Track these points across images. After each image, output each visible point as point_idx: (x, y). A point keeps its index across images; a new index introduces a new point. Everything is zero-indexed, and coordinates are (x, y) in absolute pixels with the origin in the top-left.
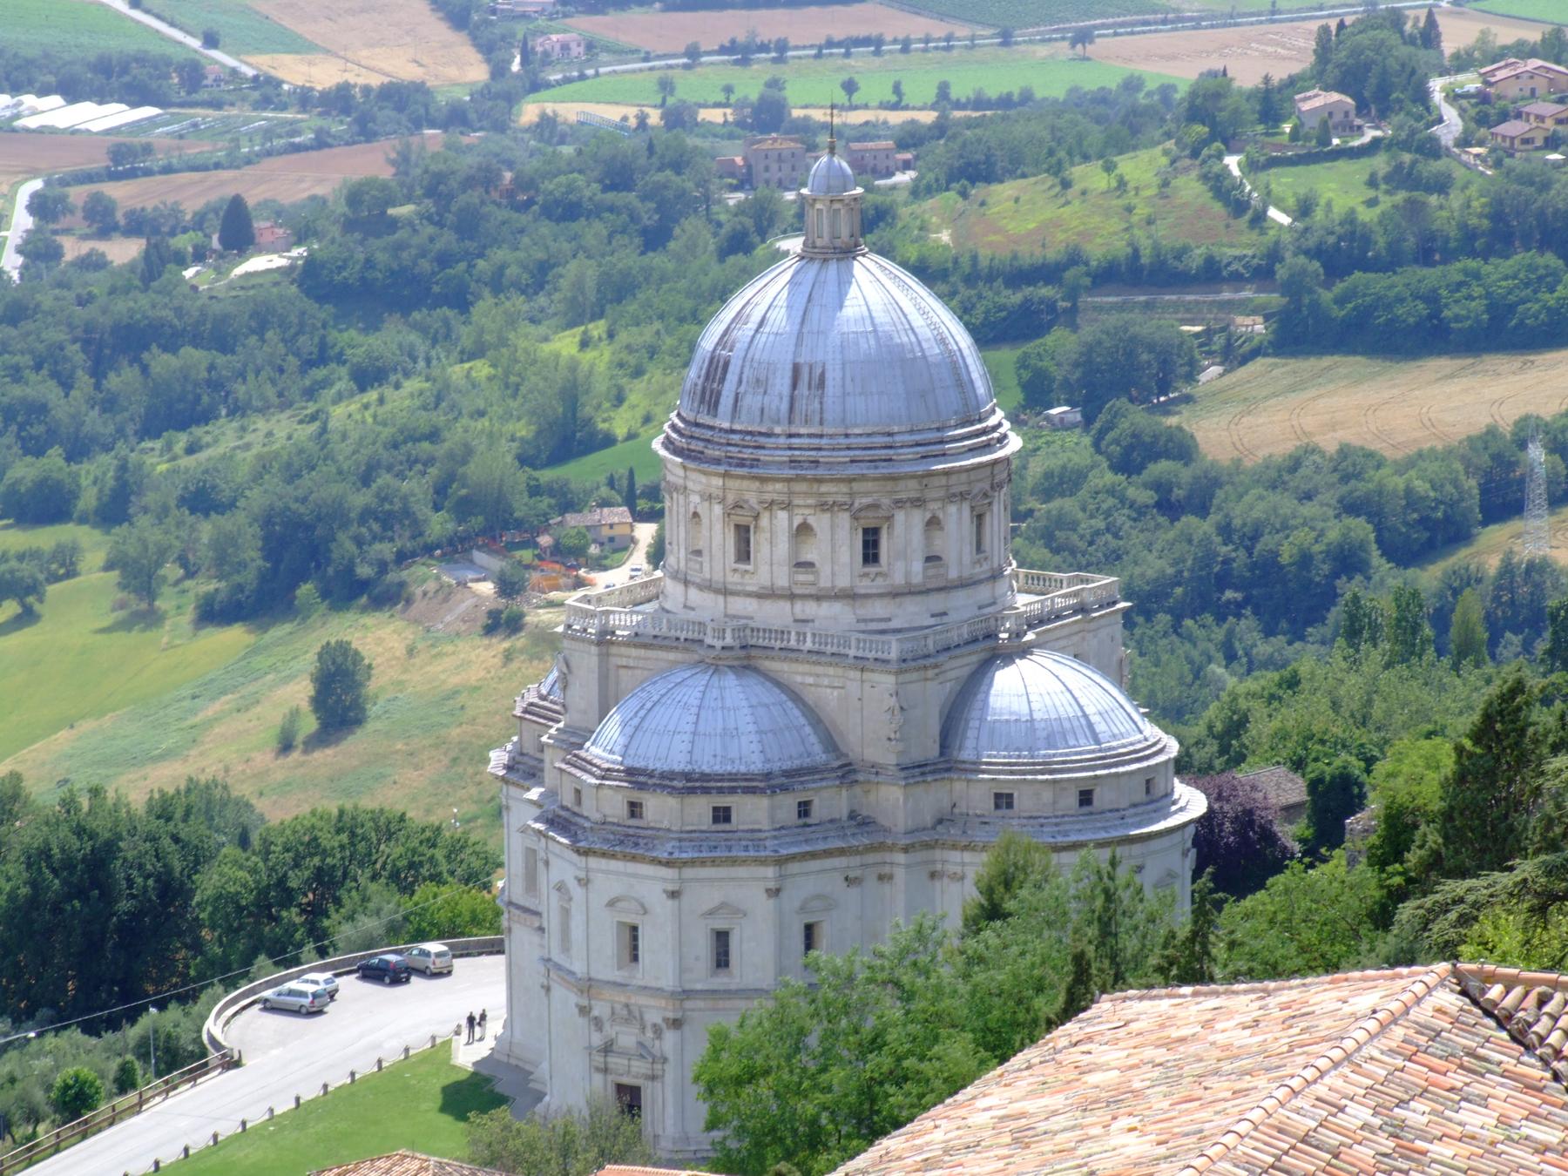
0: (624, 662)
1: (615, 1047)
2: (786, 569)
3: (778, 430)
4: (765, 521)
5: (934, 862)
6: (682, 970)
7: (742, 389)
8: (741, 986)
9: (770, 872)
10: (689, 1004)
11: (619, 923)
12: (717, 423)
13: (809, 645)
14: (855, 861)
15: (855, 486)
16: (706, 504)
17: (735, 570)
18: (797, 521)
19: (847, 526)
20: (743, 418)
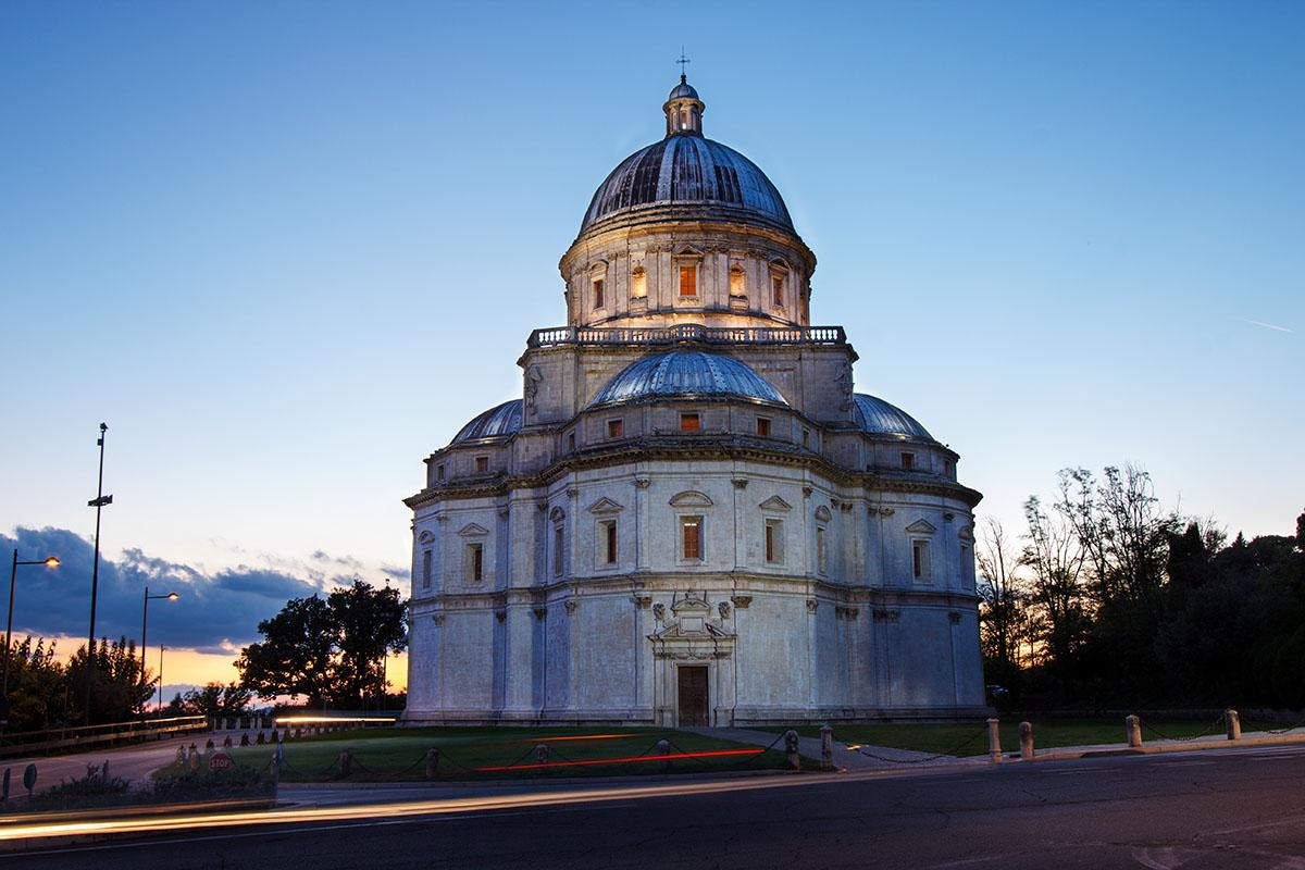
0: (593, 367)
2: (726, 297)
3: (712, 202)
4: (709, 261)
5: (871, 501)
6: (750, 554)
7: (677, 181)
8: (788, 573)
9: (807, 474)
10: (754, 585)
12: (658, 203)
14: (835, 488)
17: (682, 300)
19: (765, 270)
20: (681, 195)
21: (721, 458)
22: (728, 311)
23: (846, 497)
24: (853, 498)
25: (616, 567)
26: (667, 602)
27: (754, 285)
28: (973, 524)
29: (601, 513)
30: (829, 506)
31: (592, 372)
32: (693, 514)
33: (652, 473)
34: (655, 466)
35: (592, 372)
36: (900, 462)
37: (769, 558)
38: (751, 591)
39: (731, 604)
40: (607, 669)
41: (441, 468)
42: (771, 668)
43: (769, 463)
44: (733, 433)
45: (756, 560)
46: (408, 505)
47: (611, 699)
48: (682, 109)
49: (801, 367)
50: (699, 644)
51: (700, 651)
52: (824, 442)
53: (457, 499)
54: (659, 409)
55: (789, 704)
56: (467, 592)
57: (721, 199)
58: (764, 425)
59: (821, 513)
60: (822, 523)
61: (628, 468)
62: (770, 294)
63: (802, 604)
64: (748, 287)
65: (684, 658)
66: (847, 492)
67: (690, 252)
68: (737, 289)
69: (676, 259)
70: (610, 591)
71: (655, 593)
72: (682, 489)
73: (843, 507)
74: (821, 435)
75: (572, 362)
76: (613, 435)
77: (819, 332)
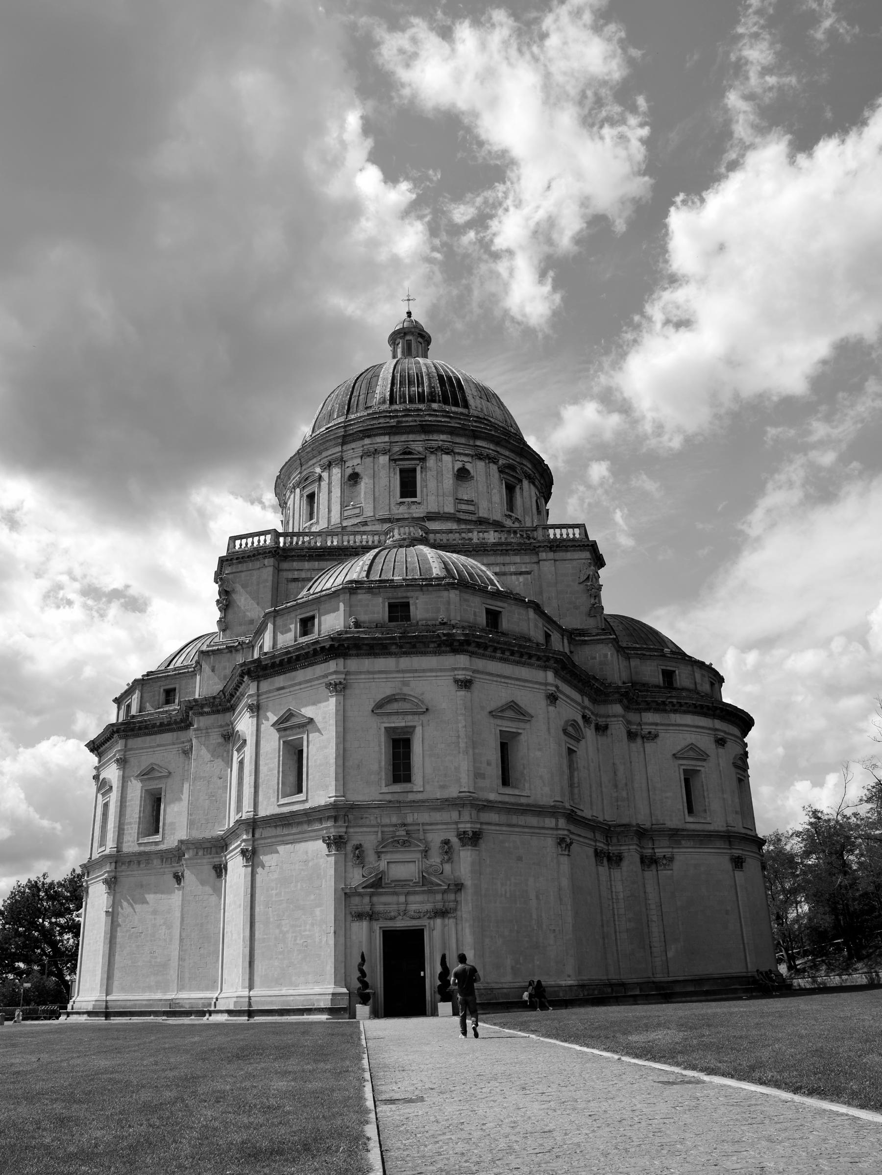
0: (296, 575)
1: (385, 881)
2: (451, 499)
4: (431, 461)
5: (629, 722)
6: (478, 775)
8: (530, 801)
10: (486, 816)
11: (385, 728)
13: (492, 540)
14: (587, 702)
15: (498, 449)
16: (371, 459)
18: (458, 465)
19: (497, 475)
21: (438, 652)
23: (601, 716)
24: (609, 716)
25: (305, 798)
26: (369, 840)
27: (482, 487)
28: (746, 754)
29: (285, 729)
31: (295, 580)
32: (403, 724)
33: (347, 673)
34: (353, 664)
35: (295, 580)
36: (659, 679)
37: (506, 781)
38: (482, 823)
39: (454, 840)
40: (289, 936)
41: (129, 707)
44: (453, 622)
46: (92, 751)
47: (294, 979)
48: (408, 338)
49: (539, 569)
50: (411, 898)
51: (413, 907)
52: (571, 652)
53: (138, 736)
54: (360, 597)
56: (142, 849)
57: (445, 401)
58: (493, 617)
59: (570, 729)
60: (572, 742)
61: (319, 669)
62: (501, 499)
63: (550, 842)
65: (392, 919)
66: (602, 709)
67: (410, 453)
69: (395, 460)
70: (294, 830)
71: (351, 830)
72: (389, 692)
74: (566, 641)
75: (271, 569)
76: (305, 632)
77: (558, 531)
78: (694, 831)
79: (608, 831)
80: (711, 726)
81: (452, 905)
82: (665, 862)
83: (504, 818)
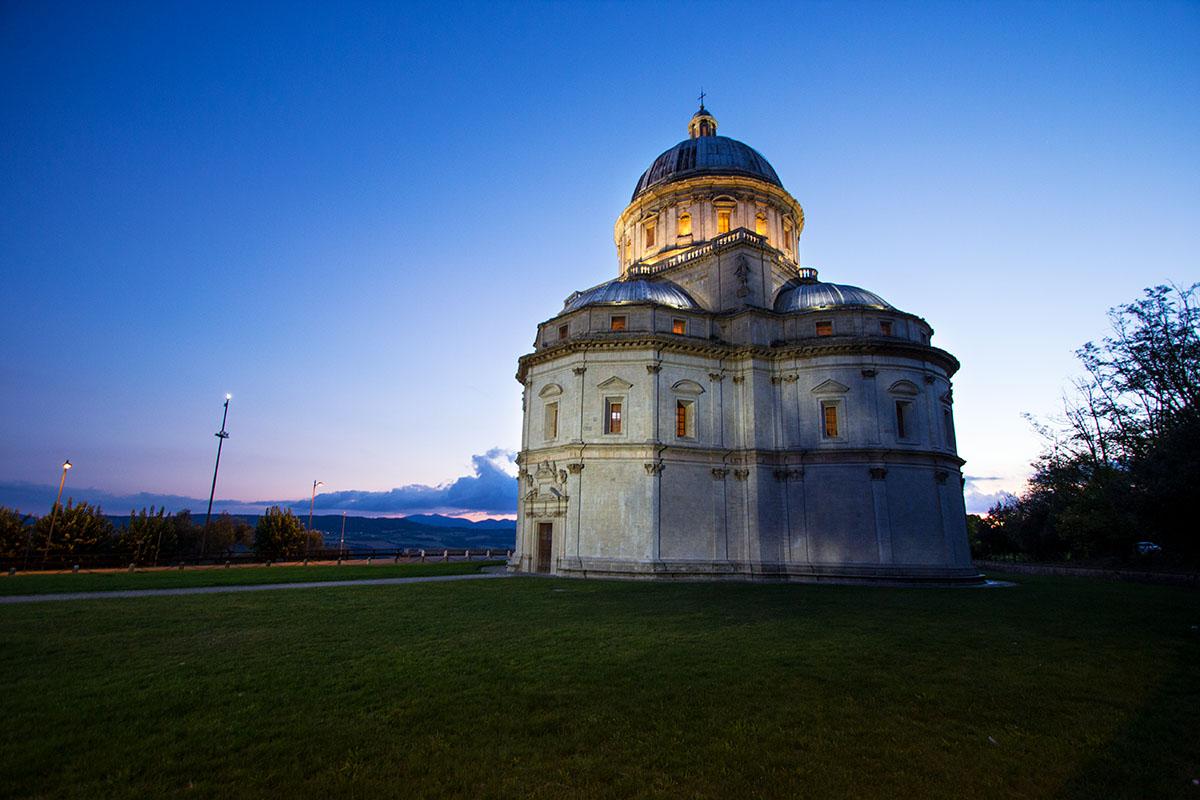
4: (662, 218)
6: (584, 428)
9: (650, 354)
10: (586, 454)
22: (676, 247)
30: (704, 380)
34: (537, 370)
39: (568, 471)
42: (603, 526)
43: (609, 350)
45: (592, 433)
55: (622, 557)
63: (641, 467)
64: (693, 226)
68: (686, 231)
73: (735, 380)
78: (827, 450)
79: (731, 454)
80: (858, 362)
81: (564, 510)
82: (795, 475)
83: (603, 454)
